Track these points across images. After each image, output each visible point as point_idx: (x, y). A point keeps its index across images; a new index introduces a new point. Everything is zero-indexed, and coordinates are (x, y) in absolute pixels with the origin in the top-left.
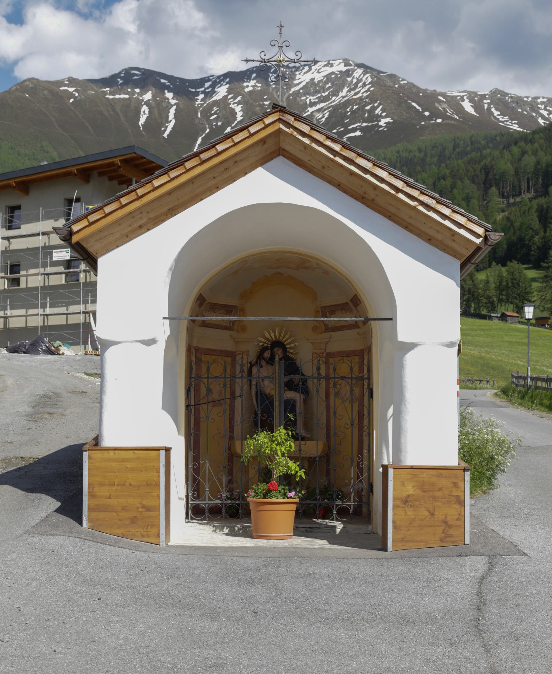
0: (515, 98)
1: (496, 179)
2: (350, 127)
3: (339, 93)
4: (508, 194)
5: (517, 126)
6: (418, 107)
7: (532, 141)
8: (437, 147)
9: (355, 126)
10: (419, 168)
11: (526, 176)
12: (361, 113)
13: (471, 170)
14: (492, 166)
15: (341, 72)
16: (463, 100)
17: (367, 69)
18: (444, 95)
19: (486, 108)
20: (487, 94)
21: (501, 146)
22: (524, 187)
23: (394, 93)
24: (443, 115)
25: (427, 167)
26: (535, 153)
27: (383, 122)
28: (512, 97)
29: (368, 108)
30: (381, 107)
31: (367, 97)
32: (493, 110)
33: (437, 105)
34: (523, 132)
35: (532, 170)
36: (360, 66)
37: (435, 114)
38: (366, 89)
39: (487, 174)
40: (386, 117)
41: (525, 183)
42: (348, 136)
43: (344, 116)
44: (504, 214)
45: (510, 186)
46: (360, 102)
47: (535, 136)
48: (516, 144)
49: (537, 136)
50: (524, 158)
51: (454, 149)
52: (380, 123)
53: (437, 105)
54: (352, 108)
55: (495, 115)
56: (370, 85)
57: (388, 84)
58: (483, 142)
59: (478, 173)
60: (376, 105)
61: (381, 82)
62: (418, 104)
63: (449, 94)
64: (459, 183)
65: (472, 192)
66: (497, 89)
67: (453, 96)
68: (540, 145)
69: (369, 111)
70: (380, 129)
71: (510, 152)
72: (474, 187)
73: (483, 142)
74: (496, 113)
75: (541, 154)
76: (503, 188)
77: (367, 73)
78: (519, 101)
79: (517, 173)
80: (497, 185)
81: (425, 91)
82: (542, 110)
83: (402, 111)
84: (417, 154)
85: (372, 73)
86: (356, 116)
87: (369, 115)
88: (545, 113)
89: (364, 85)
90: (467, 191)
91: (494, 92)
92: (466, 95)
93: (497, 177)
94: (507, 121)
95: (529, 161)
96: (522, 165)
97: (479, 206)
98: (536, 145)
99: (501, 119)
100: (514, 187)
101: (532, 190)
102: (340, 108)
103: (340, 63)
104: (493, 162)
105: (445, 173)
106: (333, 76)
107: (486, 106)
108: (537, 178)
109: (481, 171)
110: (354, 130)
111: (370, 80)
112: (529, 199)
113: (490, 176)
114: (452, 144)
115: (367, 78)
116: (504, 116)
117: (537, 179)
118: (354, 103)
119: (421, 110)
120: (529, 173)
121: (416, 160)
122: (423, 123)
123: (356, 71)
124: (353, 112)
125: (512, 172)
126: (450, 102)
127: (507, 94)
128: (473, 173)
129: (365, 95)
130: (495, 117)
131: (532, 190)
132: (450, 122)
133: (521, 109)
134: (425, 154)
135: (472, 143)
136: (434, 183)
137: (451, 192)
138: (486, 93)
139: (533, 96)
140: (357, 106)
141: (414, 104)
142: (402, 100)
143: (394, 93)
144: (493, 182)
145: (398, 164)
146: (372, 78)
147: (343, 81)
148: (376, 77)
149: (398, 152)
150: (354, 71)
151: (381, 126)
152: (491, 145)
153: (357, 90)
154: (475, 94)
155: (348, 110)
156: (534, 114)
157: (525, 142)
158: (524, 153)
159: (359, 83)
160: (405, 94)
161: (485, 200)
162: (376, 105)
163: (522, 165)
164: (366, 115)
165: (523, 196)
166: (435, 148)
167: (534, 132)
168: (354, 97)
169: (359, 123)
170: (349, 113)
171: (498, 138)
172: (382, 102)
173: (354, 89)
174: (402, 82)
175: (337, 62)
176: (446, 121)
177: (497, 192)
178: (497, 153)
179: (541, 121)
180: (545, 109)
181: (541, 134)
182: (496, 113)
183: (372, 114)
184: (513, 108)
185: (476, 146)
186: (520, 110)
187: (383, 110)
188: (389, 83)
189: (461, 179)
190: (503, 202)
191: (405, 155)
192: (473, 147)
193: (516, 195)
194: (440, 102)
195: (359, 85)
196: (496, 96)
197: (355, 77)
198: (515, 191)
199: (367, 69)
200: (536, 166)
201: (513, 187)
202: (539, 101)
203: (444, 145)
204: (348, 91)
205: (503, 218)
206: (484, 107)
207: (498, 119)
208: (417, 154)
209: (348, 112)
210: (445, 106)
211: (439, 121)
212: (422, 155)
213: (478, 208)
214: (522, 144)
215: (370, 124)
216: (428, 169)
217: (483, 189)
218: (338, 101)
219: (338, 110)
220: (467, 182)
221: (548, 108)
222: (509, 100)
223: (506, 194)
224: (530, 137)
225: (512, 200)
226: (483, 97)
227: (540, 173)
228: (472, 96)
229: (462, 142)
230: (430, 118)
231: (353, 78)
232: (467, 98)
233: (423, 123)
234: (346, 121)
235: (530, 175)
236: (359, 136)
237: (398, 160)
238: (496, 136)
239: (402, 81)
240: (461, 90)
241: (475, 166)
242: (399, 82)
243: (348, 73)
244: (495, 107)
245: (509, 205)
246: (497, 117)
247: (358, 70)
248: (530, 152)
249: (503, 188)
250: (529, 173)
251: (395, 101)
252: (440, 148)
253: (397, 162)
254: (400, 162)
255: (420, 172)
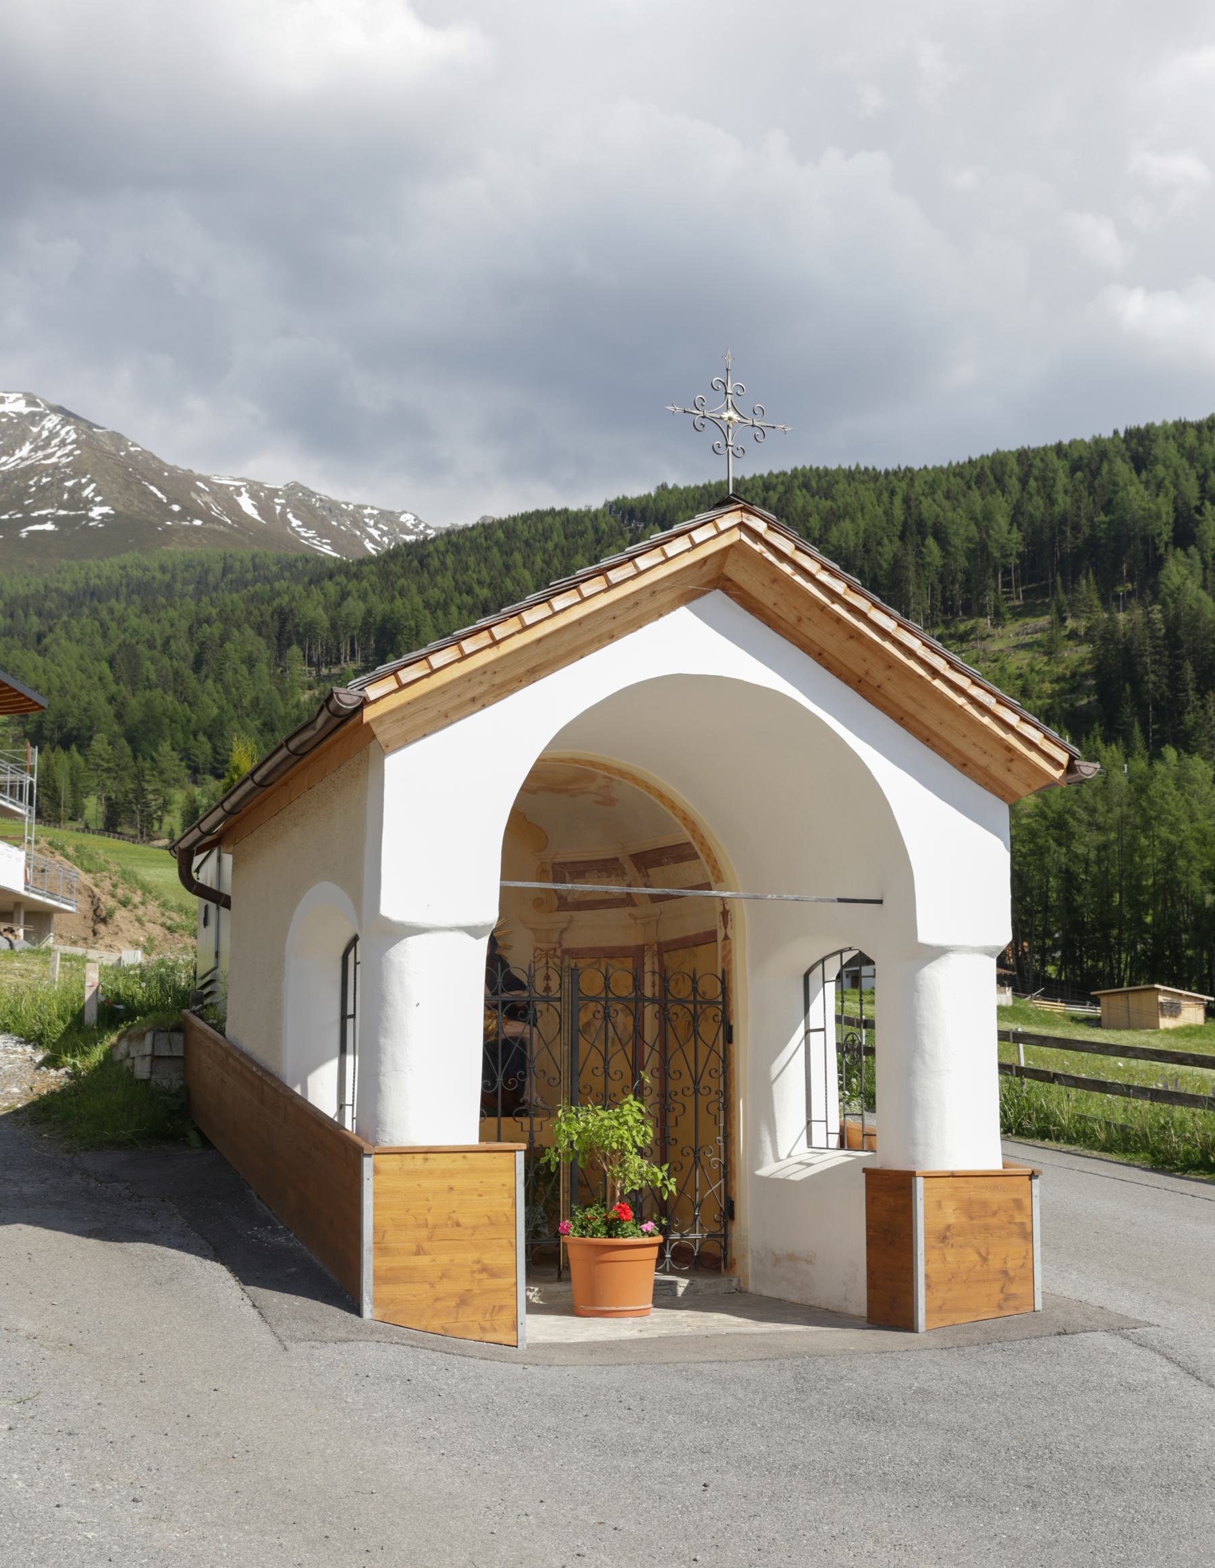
0: (327, 502)
1: (298, 632)
2: (35, 514)
3: (14, 451)
4: (318, 660)
5: (329, 547)
6: (160, 495)
7: (358, 576)
8: (194, 568)
9: (44, 512)
10: (162, 600)
11: (349, 634)
12: (55, 491)
13: (256, 612)
14: (291, 610)
15: (19, 415)
16: (240, 494)
17: (68, 416)
18: (206, 481)
19: (278, 512)
20: (280, 490)
21: (306, 579)
22: (346, 650)
23: (118, 465)
24: (205, 515)
25: (177, 598)
26: (363, 597)
27: (96, 512)
28: (321, 500)
29: (69, 484)
30: (93, 486)
31: (67, 465)
32: (290, 516)
33: (193, 495)
34: (340, 559)
35: (360, 624)
36: (58, 410)
37: (190, 511)
38: (67, 451)
39: (283, 622)
40: (102, 504)
41: (346, 644)
42: (30, 528)
43: (23, 493)
44: (312, 692)
45: (322, 646)
46: (53, 472)
47: (363, 569)
48: (331, 577)
49: (365, 569)
50: (345, 603)
51: (224, 574)
52: (92, 514)
53: (193, 495)
54: (40, 480)
55: (294, 525)
56: (74, 446)
57: (108, 448)
58: (274, 569)
59: (268, 619)
60: (84, 481)
61: (95, 442)
62: (160, 490)
63: (216, 480)
64: (236, 633)
65: (258, 650)
66: (296, 483)
67: (221, 485)
68: (371, 585)
69: (71, 491)
70: (91, 524)
71: (322, 589)
72: (261, 643)
73: (274, 569)
74: (295, 523)
75: (373, 599)
76: (310, 648)
77: (68, 423)
78: (333, 507)
79: (333, 626)
80: (300, 643)
81: (173, 469)
82: (370, 527)
83: (131, 498)
84: (159, 575)
85: (77, 426)
86: (45, 495)
87: (71, 497)
88: (375, 533)
89: (63, 443)
90: (249, 649)
91: (293, 488)
92: (244, 486)
93: (301, 630)
94: (313, 538)
95: (355, 608)
96: (343, 613)
97: (270, 676)
98: (365, 583)
99: (303, 534)
100: (328, 651)
101: (358, 657)
102: (17, 478)
103: (18, 399)
104: (294, 604)
105: (210, 614)
106: (4, 420)
107: (278, 508)
108: (367, 638)
109: (272, 617)
110: (42, 520)
111: (73, 436)
112: (354, 671)
113: (289, 627)
114: (221, 565)
115: (67, 433)
116: (309, 529)
117: (368, 639)
118: (42, 472)
119: (165, 501)
120: (354, 628)
121: (156, 585)
122: (169, 523)
123: (48, 418)
124: (41, 488)
125: (326, 624)
126: (216, 493)
127: (314, 494)
128: (259, 619)
129: (64, 460)
130: (293, 529)
131: (358, 657)
132: (216, 527)
133: (337, 521)
134: (173, 578)
135: (255, 568)
136: (190, 628)
137: (221, 646)
138: (279, 487)
139: (356, 503)
140: (49, 479)
141: (153, 488)
142: (132, 480)
143: (118, 465)
144: (294, 638)
145: (124, 589)
146: (77, 434)
147: (23, 430)
148: (85, 433)
149: (124, 568)
150: (43, 416)
151: (93, 520)
152: (287, 574)
153: (50, 451)
154: (261, 486)
155: (31, 483)
156: (358, 533)
157: (346, 577)
158: (344, 595)
159: (53, 439)
160: (137, 469)
161: (279, 666)
162: (84, 481)
163: (343, 613)
164: (66, 496)
165: (343, 665)
166: (191, 569)
167: (361, 562)
168: (43, 462)
169: (52, 508)
170: (33, 489)
171: (300, 565)
172: (96, 478)
173: (43, 448)
174: (132, 449)
175: (13, 396)
176: (208, 525)
177: (302, 654)
178: (298, 589)
179: (369, 546)
180: (376, 527)
181: (372, 566)
182: (295, 523)
183: (76, 496)
184: (323, 519)
185: (262, 573)
186: (334, 523)
187: (97, 492)
188: (110, 448)
189: (239, 627)
190: (310, 673)
191: (136, 573)
192: (256, 574)
193: (331, 663)
194: (199, 491)
195: (53, 443)
196: (296, 494)
197: (46, 427)
198: (331, 657)
199: (68, 416)
200: (364, 619)
201: (327, 648)
202: (366, 512)
203: (206, 566)
204: (32, 450)
205: (311, 700)
206: (275, 509)
207: (298, 533)
208: (159, 575)
209: (31, 486)
210: (208, 499)
211: (198, 522)
212: (167, 577)
213: (268, 678)
214: (341, 579)
215: (72, 513)
216: (179, 604)
217: (275, 647)
218: (13, 464)
219: (12, 481)
220: (250, 632)
221: (380, 526)
222: (318, 505)
223: (315, 660)
224: (354, 569)
225: (324, 671)
226: (274, 493)
227: (372, 631)
228: (255, 490)
229: (237, 564)
230: (182, 515)
231: (43, 428)
232: (247, 491)
233: (169, 523)
234: (27, 502)
235: (355, 633)
236: (50, 531)
237: (124, 582)
238: (296, 560)
239: (132, 446)
240: (236, 477)
241: (262, 608)
242: (127, 449)
243: (34, 418)
244: (293, 513)
245: (320, 679)
246: (297, 529)
247: (52, 416)
248: (355, 594)
249: (310, 648)
250: (354, 628)
251: (120, 480)
252: (199, 569)
253: (121, 584)
254: (128, 586)
255: (164, 607)
